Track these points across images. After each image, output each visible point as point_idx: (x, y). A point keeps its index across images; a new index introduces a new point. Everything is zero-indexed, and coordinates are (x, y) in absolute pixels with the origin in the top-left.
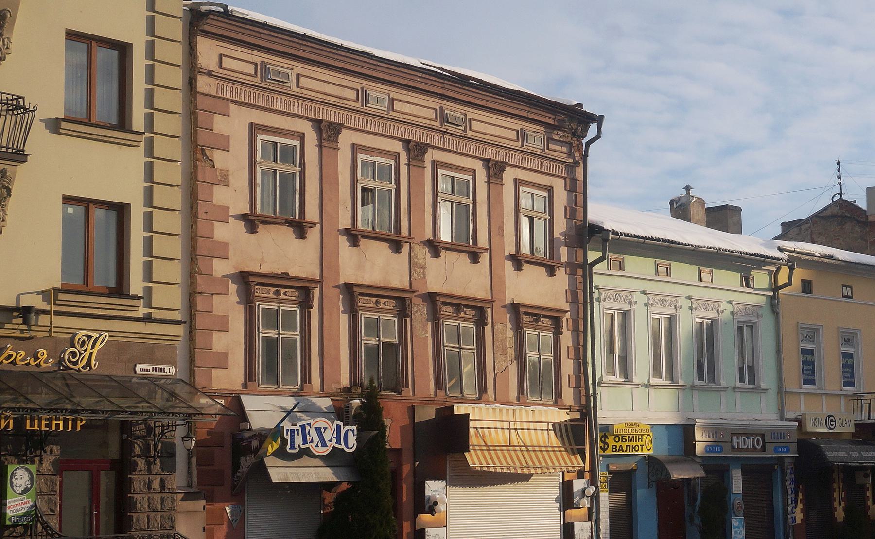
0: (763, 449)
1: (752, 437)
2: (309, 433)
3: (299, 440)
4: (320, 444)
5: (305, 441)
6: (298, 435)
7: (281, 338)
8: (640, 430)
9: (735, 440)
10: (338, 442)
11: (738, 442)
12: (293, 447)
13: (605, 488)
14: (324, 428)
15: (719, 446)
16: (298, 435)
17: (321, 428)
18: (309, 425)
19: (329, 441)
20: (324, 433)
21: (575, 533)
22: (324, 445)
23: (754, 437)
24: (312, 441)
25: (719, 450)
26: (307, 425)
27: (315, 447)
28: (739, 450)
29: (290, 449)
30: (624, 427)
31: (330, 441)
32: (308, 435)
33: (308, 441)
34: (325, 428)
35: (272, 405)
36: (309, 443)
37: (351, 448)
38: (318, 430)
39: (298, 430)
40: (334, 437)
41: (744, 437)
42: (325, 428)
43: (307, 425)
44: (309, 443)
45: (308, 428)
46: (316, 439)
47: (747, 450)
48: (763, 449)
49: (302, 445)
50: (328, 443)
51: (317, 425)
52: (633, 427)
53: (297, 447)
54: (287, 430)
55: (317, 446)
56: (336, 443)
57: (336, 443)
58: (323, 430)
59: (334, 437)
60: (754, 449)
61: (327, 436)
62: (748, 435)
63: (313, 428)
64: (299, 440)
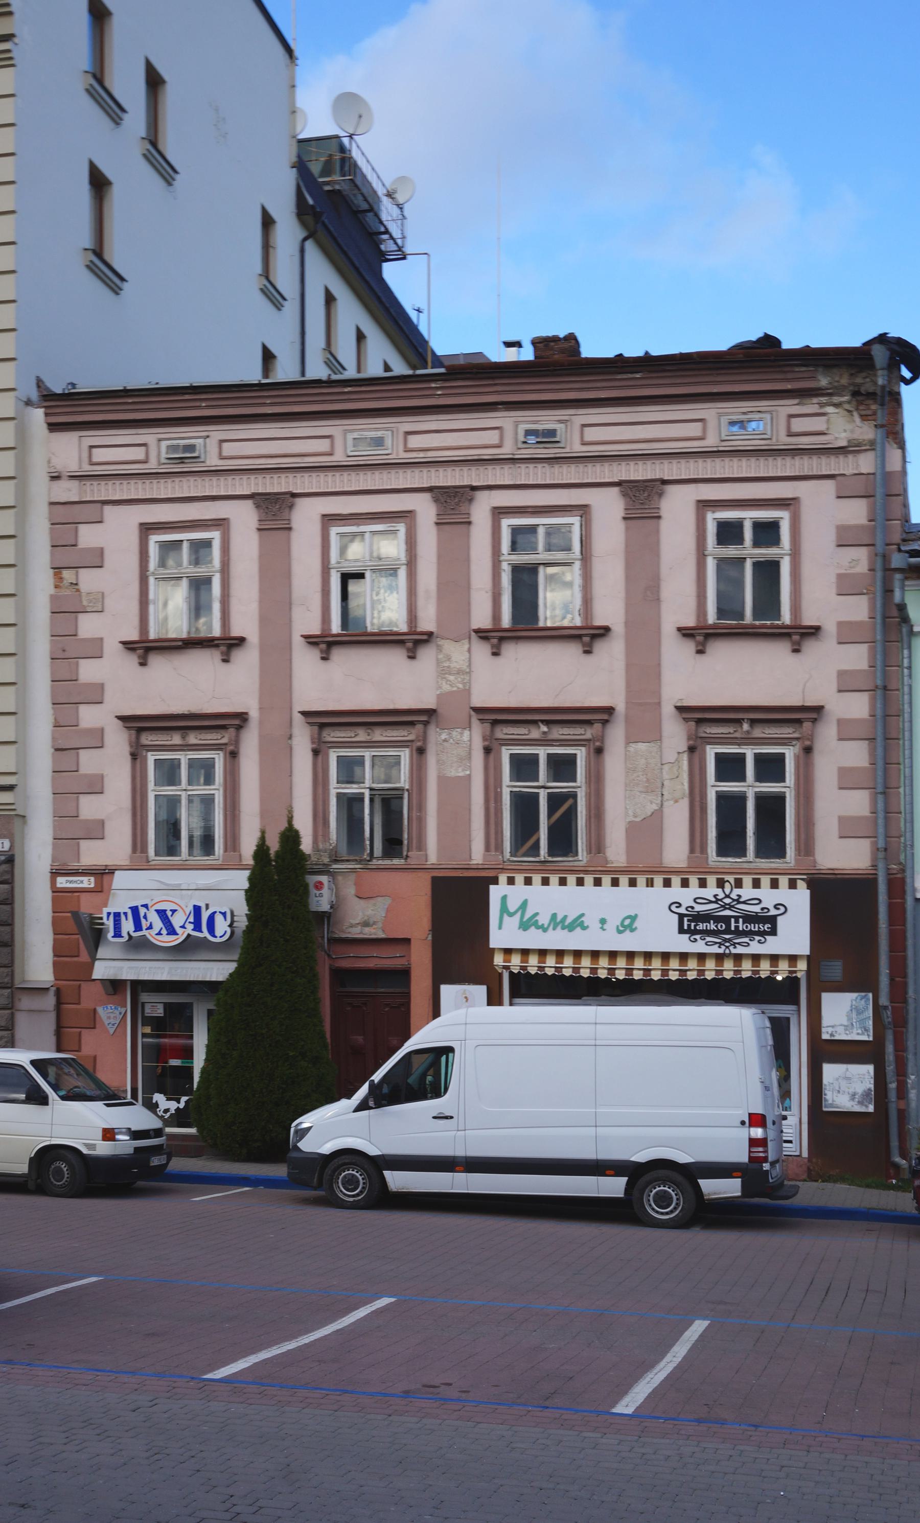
2: (145, 917)
3: (128, 926)
4: (164, 932)
5: (138, 927)
6: (127, 919)
7: (212, 792)
10: (198, 927)
12: (118, 934)
14: (171, 910)
16: (127, 919)
17: (166, 910)
18: (146, 906)
19: (181, 927)
20: (172, 916)
22: (172, 931)
24: (150, 927)
26: (142, 906)
27: (157, 934)
29: (113, 937)
31: (183, 927)
32: (143, 921)
33: (144, 927)
34: (174, 911)
35: (156, 880)
36: (146, 929)
37: (221, 937)
38: (162, 913)
39: (125, 914)
40: (190, 922)
42: (174, 911)
43: (142, 906)
44: (146, 929)
45: (142, 911)
46: (158, 924)
49: (134, 932)
50: (179, 930)
51: (161, 907)
53: (124, 933)
54: (108, 913)
55: (159, 934)
56: (193, 930)
57: (193, 930)
58: (169, 913)
59: (190, 922)
61: (177, 921)
63: (152, 910)
64: (128, 926)
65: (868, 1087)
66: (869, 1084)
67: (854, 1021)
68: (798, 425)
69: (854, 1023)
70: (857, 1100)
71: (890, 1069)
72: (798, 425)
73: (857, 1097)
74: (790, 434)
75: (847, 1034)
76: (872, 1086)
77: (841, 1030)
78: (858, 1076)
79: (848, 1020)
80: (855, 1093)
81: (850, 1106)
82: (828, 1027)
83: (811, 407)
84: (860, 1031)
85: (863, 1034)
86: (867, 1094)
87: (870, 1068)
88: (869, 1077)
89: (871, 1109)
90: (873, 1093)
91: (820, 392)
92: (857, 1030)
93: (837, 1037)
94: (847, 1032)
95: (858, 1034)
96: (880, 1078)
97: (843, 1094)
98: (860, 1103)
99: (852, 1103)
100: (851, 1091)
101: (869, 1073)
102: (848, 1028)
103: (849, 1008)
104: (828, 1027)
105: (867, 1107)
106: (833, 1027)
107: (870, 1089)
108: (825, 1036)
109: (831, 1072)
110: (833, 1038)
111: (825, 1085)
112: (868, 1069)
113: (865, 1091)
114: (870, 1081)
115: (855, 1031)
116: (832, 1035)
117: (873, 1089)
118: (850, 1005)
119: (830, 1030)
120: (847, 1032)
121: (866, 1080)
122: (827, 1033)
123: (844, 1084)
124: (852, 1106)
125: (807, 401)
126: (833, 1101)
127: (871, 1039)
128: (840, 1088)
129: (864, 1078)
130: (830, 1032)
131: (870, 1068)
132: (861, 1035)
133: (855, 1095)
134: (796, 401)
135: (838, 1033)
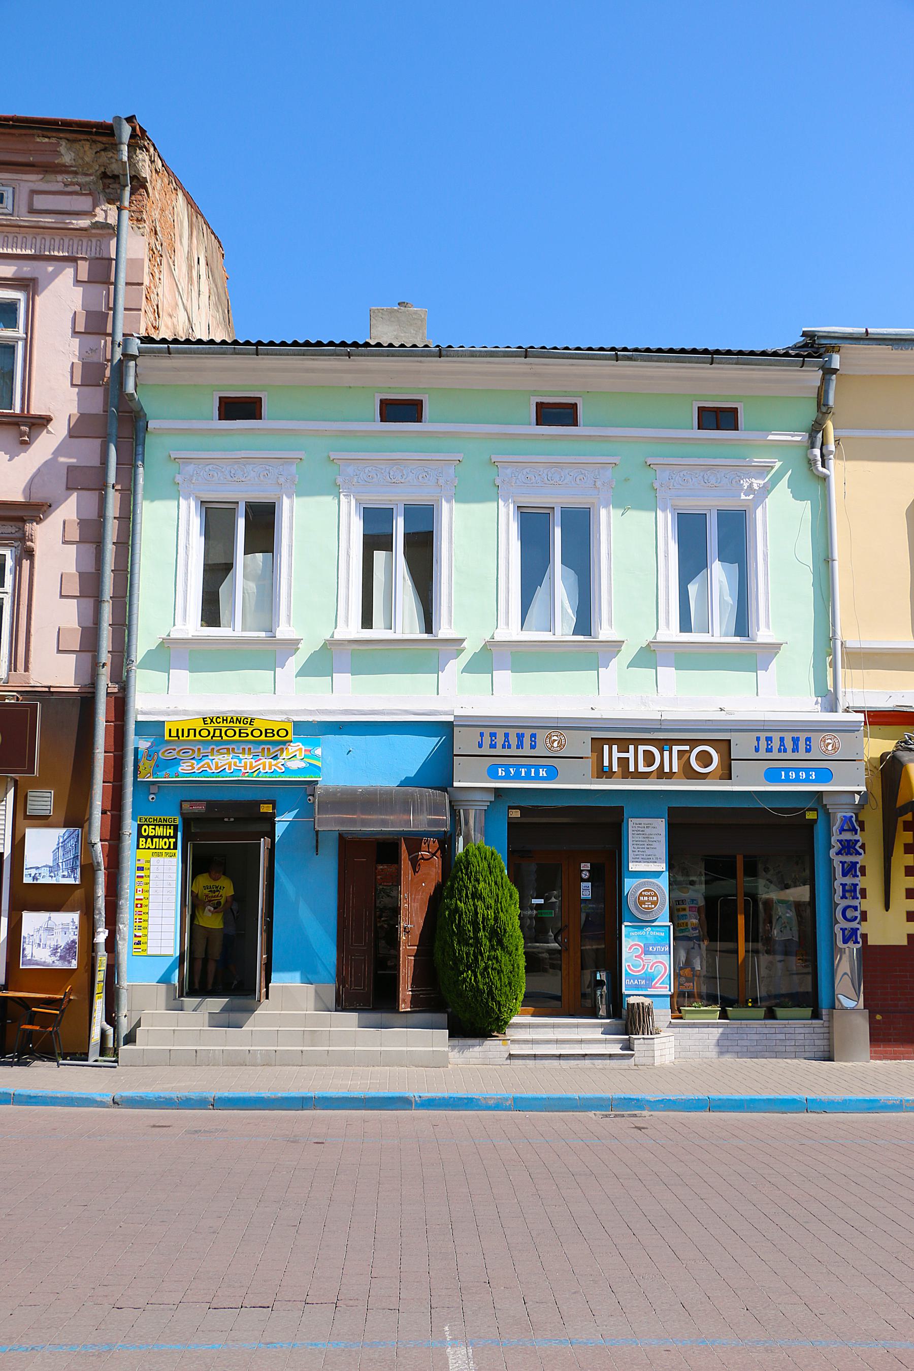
0: (727, 775)
1: (676, 749)
8: (256, 733)
9: (612, 756)
11: (623, 762)
13: (169, 848)
15: (543, 766)
21: (24, 932)
23: (687, 748)
25: (542, 773)
28: (626, 774)
30: (199, 725)
41: (641, 748)
47: (661, 774)
48: (727, 775)
52: (232, 724)
60: (689, 773)
62: (663, 744)
65: (71, 939)
66: (73, 935)
67: (61, 861)
68: (41, 202)
69: (60, 864)
70: (59, 954)
71: (101, 917)
72: (41, 202)
73: (59, 950)
74: (32, 211)
75: (52, 877)
76: (76, 937)
77: (45, 872)
78: (61, 926)
79: (54, 860)
80: (57, 946)
81: (51, 962)
82: (31, 868)
83: (57, 182)
84: (66, 873)
85: (69, 876)
86: (70, 947)
87: (75, 916)
88: (75, 927)
89: (74, 964)
90: (77, 946)
91: (67, 169)
92: (63, 872)
93: (41, 881)
94: (52, 874)
95: (64, 876)
96: (88, 928)
97: (43, 948)
98: (62, 958)
99: (53, 958)
100: (53, 943)
101: (73, 922)
102: (52, 869)
103: (56, 846)
104: (31, 868)
105: (70, 962)
106: (37, 868)
107: (73, 942)
108: (27, 880)
109: (31, 921)
110: (35, 882)
111: (24, 938)
112: (71, 919)
113: (67, 944)
114: (74, 932)
115: (61, 873)
116: (34, 878)
117: (77, 941)
118: (57, 843)
119: (33, 872)
120: (52, 874)
121: (70, 930)
122: (30, 875)
123: (44, 935)
124: (53, 962)
125: (51, 177)
126: (32, 956)
127: (77, 883)
128: (41, 940)
129: (68, 929)
130: (33, 875)
131: (75, 916)
132: (67, 877)
133: (57, 949)
134: (41, 176)
135: (42, 874)
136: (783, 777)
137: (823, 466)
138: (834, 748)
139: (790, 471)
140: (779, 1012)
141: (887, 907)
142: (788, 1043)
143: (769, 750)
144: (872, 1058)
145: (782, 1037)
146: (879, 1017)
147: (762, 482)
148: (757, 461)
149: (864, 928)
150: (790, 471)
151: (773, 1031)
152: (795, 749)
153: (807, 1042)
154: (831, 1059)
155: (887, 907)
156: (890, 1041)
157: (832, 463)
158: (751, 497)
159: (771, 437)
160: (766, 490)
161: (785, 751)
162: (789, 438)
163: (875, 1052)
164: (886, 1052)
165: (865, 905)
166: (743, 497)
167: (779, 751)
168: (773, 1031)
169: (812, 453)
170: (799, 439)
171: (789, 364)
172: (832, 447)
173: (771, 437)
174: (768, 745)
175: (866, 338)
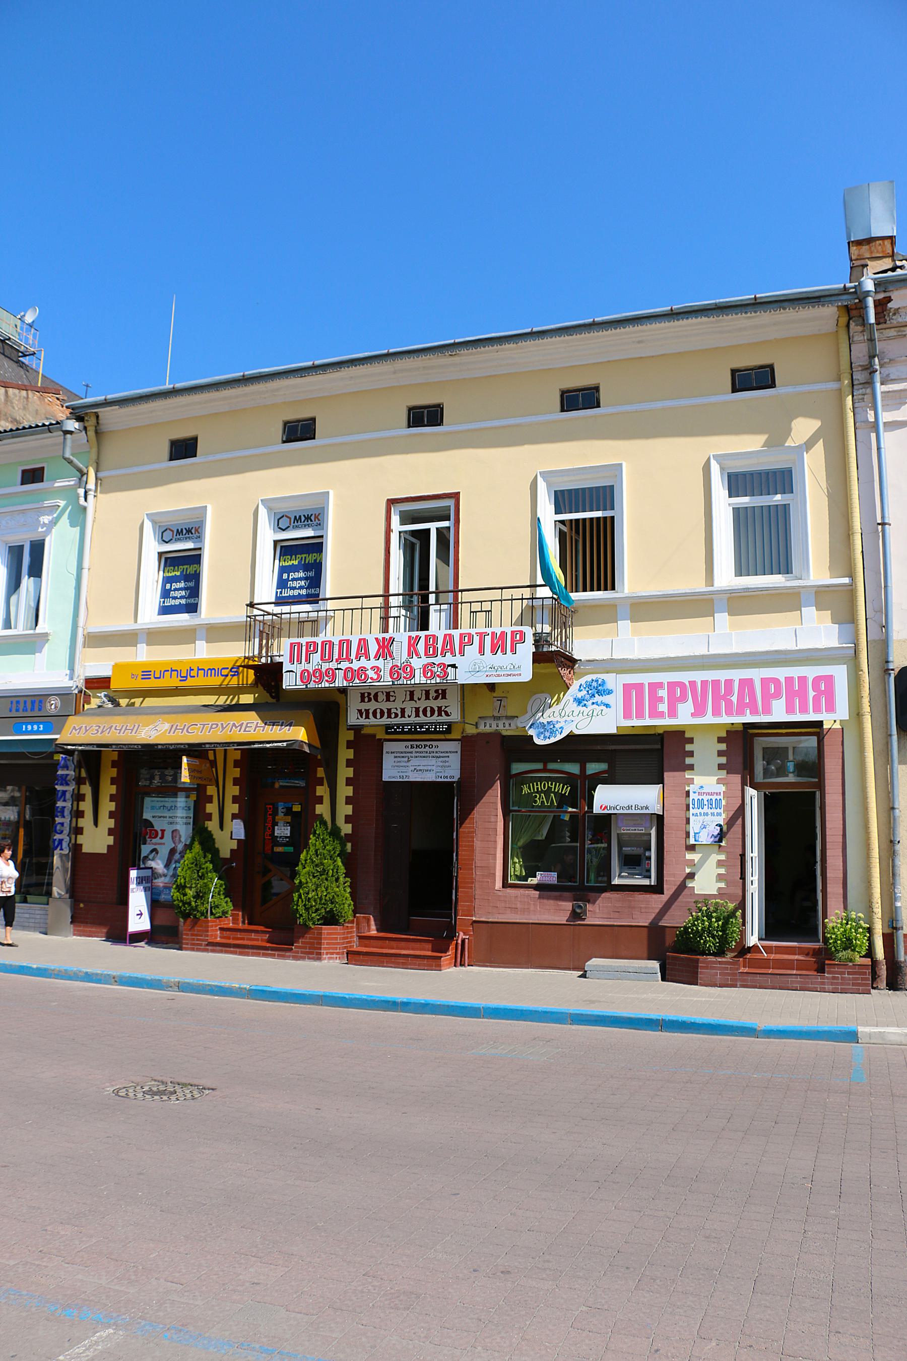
136: (24, 730)
137: (86, 500)
138: (56, 707)
139: (70, 507)
140: (29, 898)
141: (96, 824)
142: (31, 920)
143: (17, 710)
144: (74, 935)
145: (27, 916)
146: (82, 905)
147: (50, 518)
148: (47, 503)
149: (81, 839)
150: (70, 507)
151: (22, 911)
152: (32, 709)
153: (42, 921)
154: (46, 934)
155: (96, 824)
156: (87, 923)
157: (90, 497)
158: (45, 528)
159: (57, 485)
160: (54, 523)
161: (26, 711)
162: (67, 483)
163: (78, 931)
164: (84, 931)
165: (82, 823)
166: (40, 530)
167: (23, 711)
168: (22, 911)
169: (76, 491)
170: (72, 483)
171: (42, 432)
172: (91, 485)
173: (57, 485)
174: (17, 706)
175: (107, 403)
